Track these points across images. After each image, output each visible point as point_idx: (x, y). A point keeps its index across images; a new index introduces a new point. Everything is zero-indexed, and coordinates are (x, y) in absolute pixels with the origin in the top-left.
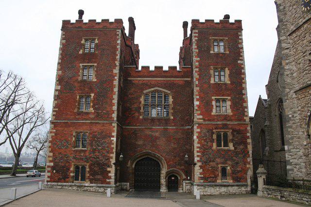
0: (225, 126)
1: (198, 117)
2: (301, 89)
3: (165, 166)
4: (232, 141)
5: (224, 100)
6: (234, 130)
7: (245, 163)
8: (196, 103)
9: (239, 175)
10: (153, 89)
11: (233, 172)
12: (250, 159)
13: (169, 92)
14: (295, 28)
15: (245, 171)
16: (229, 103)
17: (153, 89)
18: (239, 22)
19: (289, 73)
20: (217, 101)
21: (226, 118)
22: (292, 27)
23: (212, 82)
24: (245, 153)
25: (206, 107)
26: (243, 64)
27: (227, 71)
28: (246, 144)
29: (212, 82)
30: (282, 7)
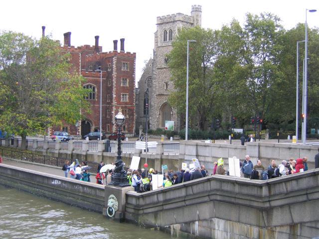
0: (126, 107)
1: (114, 103)
2: (159, 95)
3: (94, 125)
4: (128, 114)
5: (126, 95)
6: (129, 109)
7: (133, 124)
8: (114, 96)
9: (130, 129)
10: (87, 84)
11: (128, 128)
12: (134, 122)
13: (95, 86)
14: (160, 67)
15: (132, 127)
16: (127, 96)
17: (87, 84)
18: (135, 54)
19: (154, 86)
20: (123, 95)
21: (126, 103)
22: (159, 66)
23: (122, 85)
24: (133, 119)
25: (118, 98)
26: (135, 77)
27: (128, 80)
28: (133, 115)
29: (122, 85)
30: (156, 54)
